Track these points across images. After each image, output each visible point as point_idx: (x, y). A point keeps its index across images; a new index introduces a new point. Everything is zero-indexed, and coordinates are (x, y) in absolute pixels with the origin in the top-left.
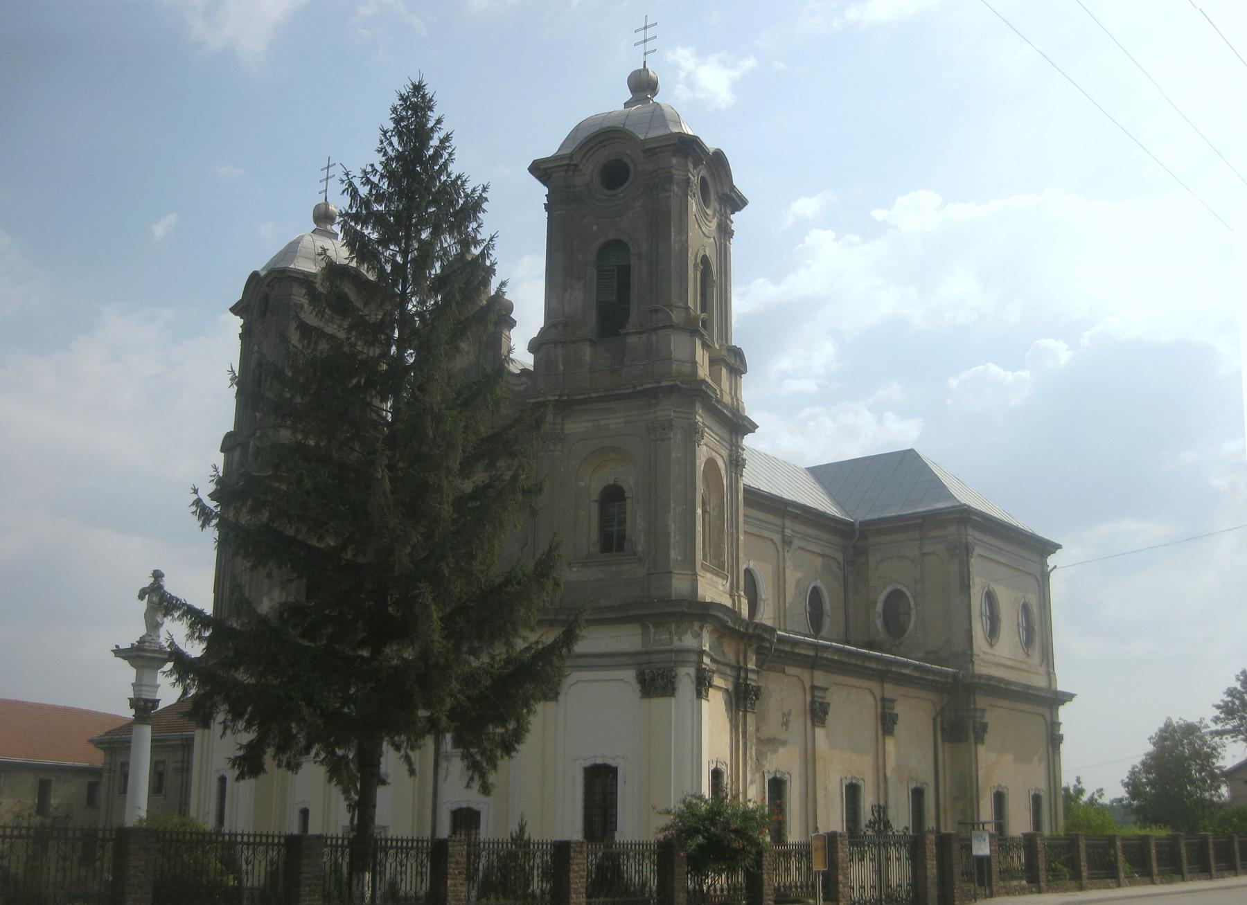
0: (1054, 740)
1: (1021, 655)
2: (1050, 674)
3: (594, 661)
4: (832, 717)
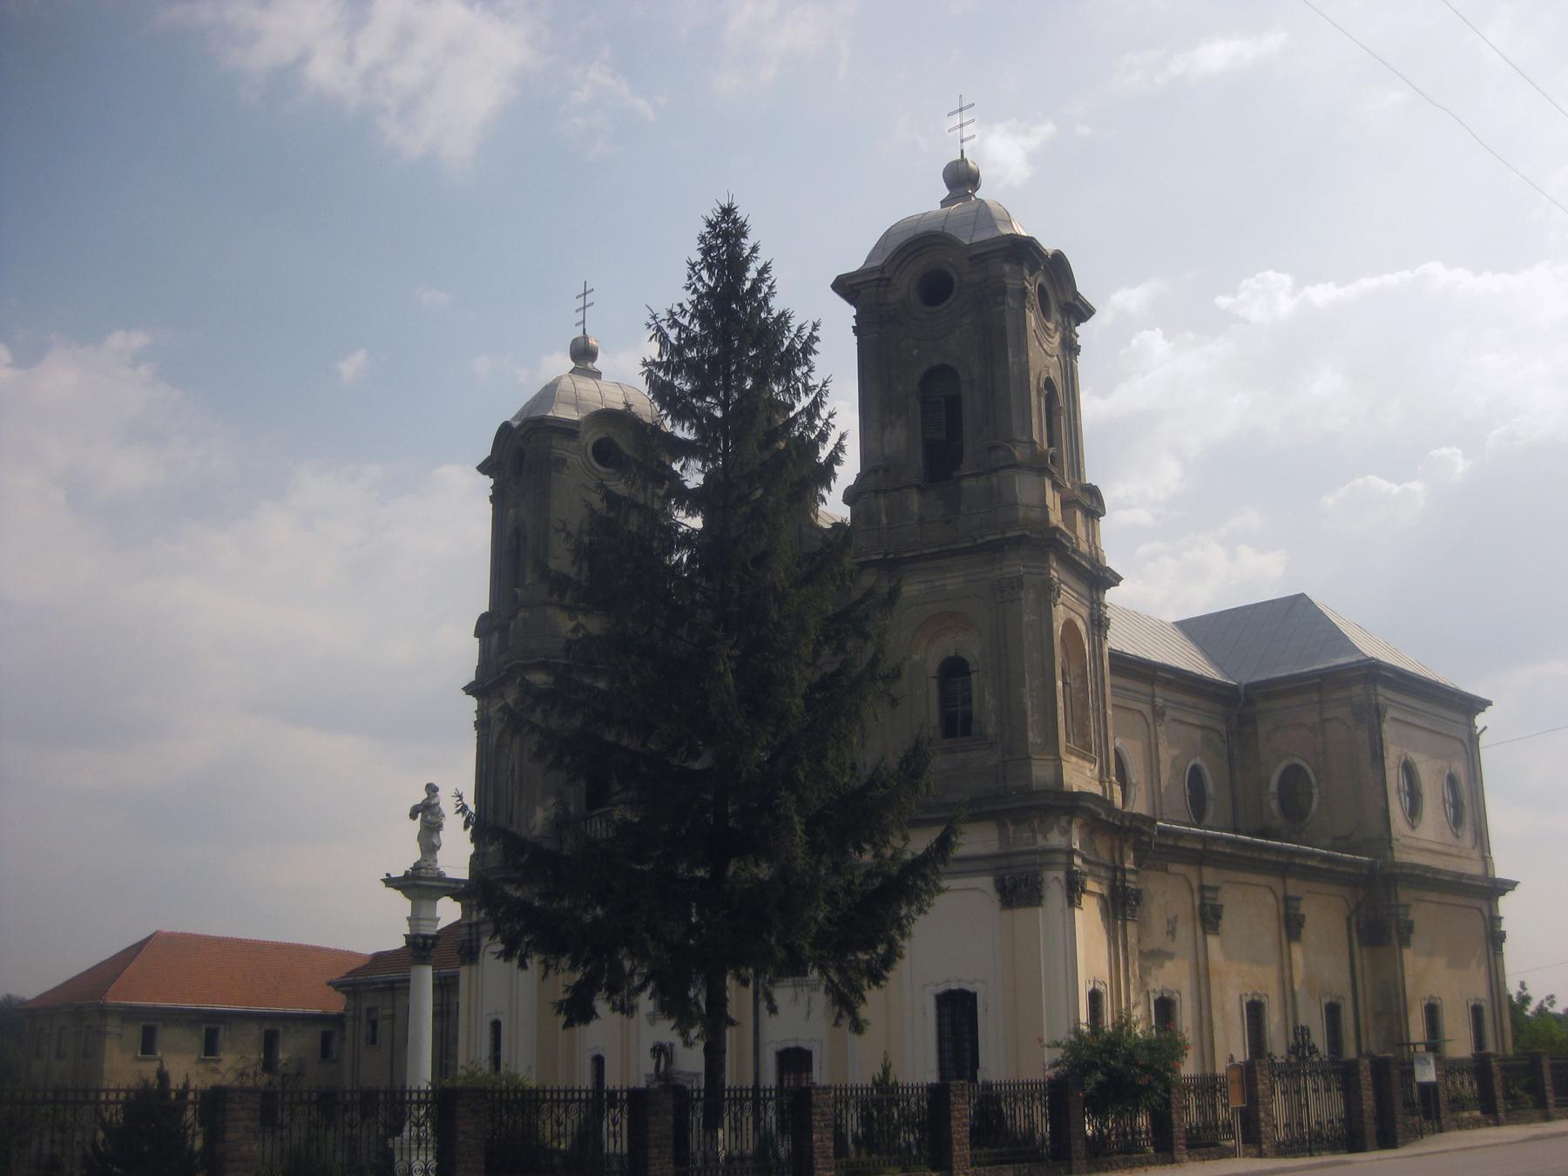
0: (1495, 939)
1: (1449, 837)
2: (1486, 859)
4: (1225, 923)
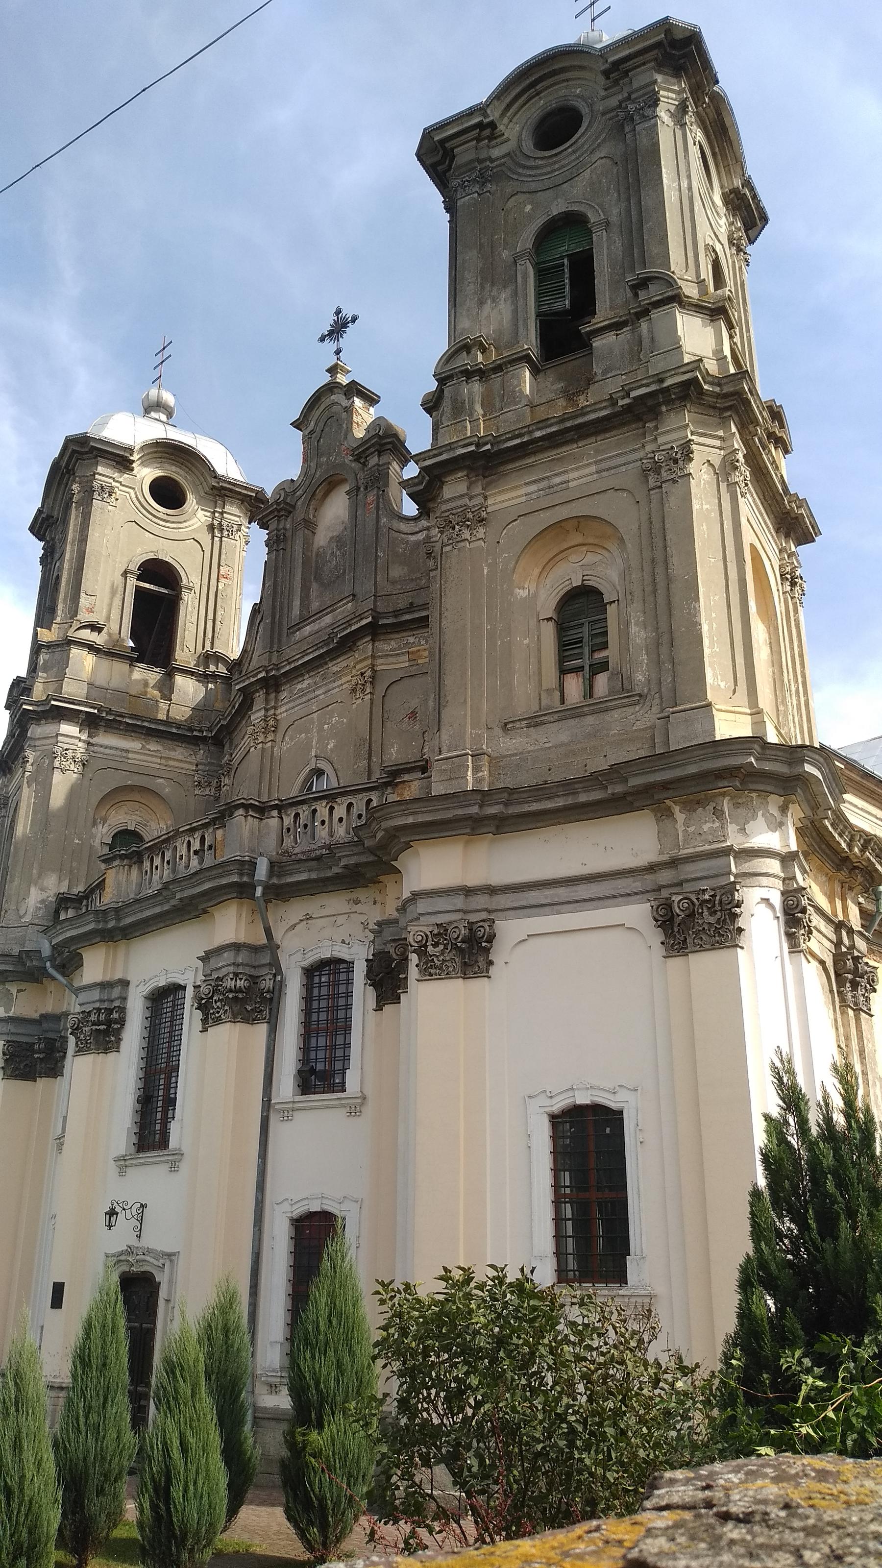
3: (563, 893)
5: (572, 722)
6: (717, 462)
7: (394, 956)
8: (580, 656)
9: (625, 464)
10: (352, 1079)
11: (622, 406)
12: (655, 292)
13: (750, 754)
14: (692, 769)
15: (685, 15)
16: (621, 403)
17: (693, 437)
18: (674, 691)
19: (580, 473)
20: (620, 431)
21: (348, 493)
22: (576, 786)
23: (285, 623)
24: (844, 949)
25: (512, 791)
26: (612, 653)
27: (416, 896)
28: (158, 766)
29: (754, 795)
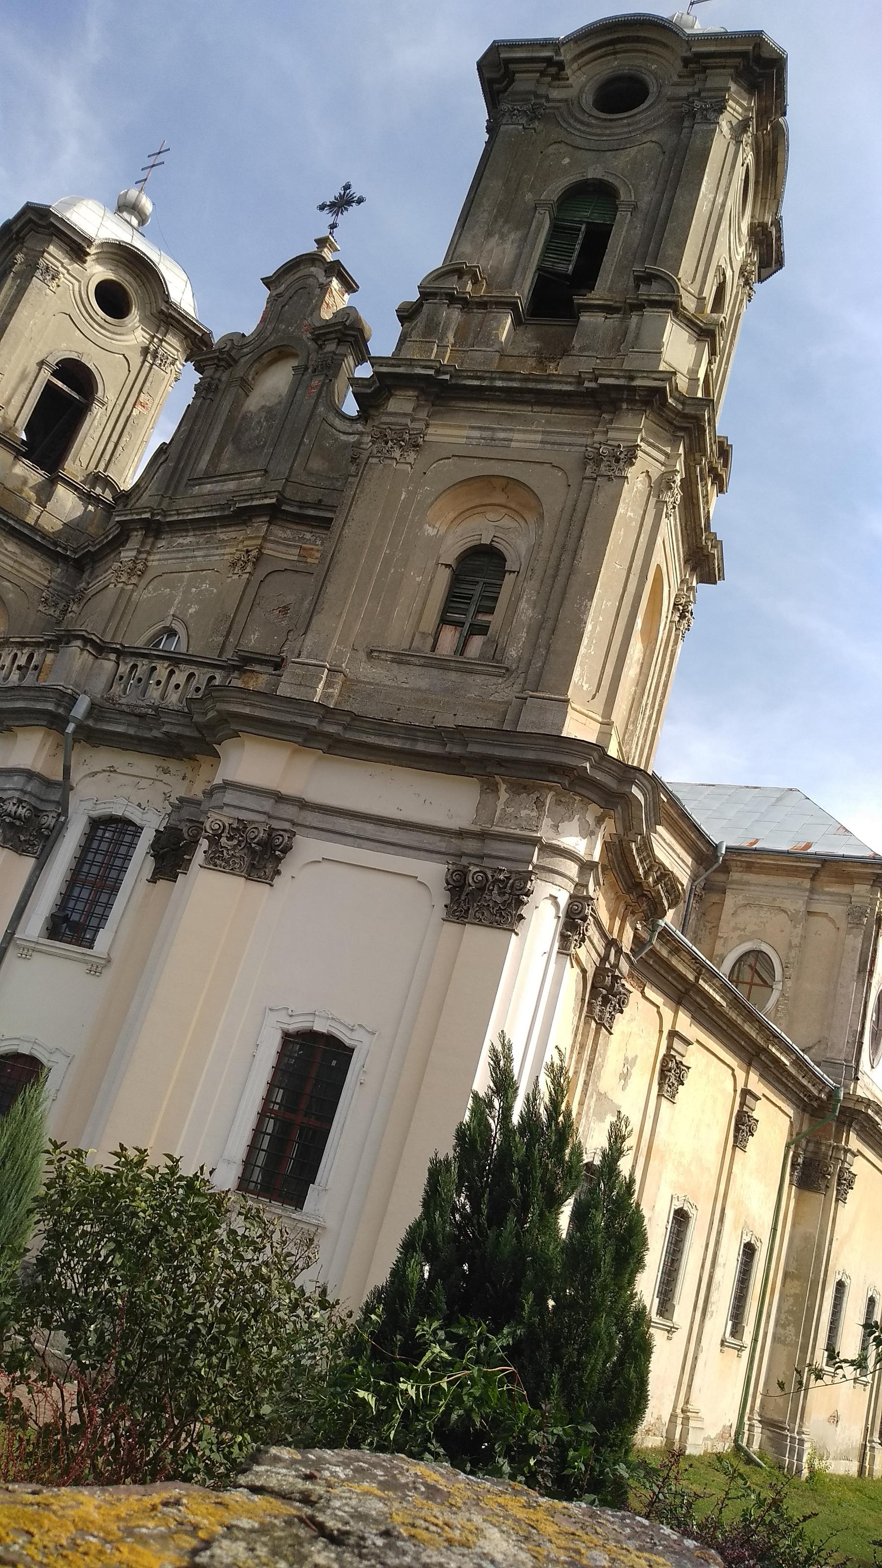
3: (369, 829)
5: (435, 672)
6: (655, 476)
7: (186, 836)
8: (465, 612)
9: (570, 445)
10: (103, 939)
11: (587, 388)
12: (655, 291)
13: (588, 760)
14: (530, 755)
15: (778, 36)
16: (587, 384)
17: (642, 444)
18: (540, 676)
19: (526, 438)
20: (576, 412)
21: (294, 369)
22: (418, 734)
23: (187, 473)
24: (608, 966)
25: (355, 717)
26: (495, 620)
27: (227, 785)
28: (9, 569)
29: (578, 798)
